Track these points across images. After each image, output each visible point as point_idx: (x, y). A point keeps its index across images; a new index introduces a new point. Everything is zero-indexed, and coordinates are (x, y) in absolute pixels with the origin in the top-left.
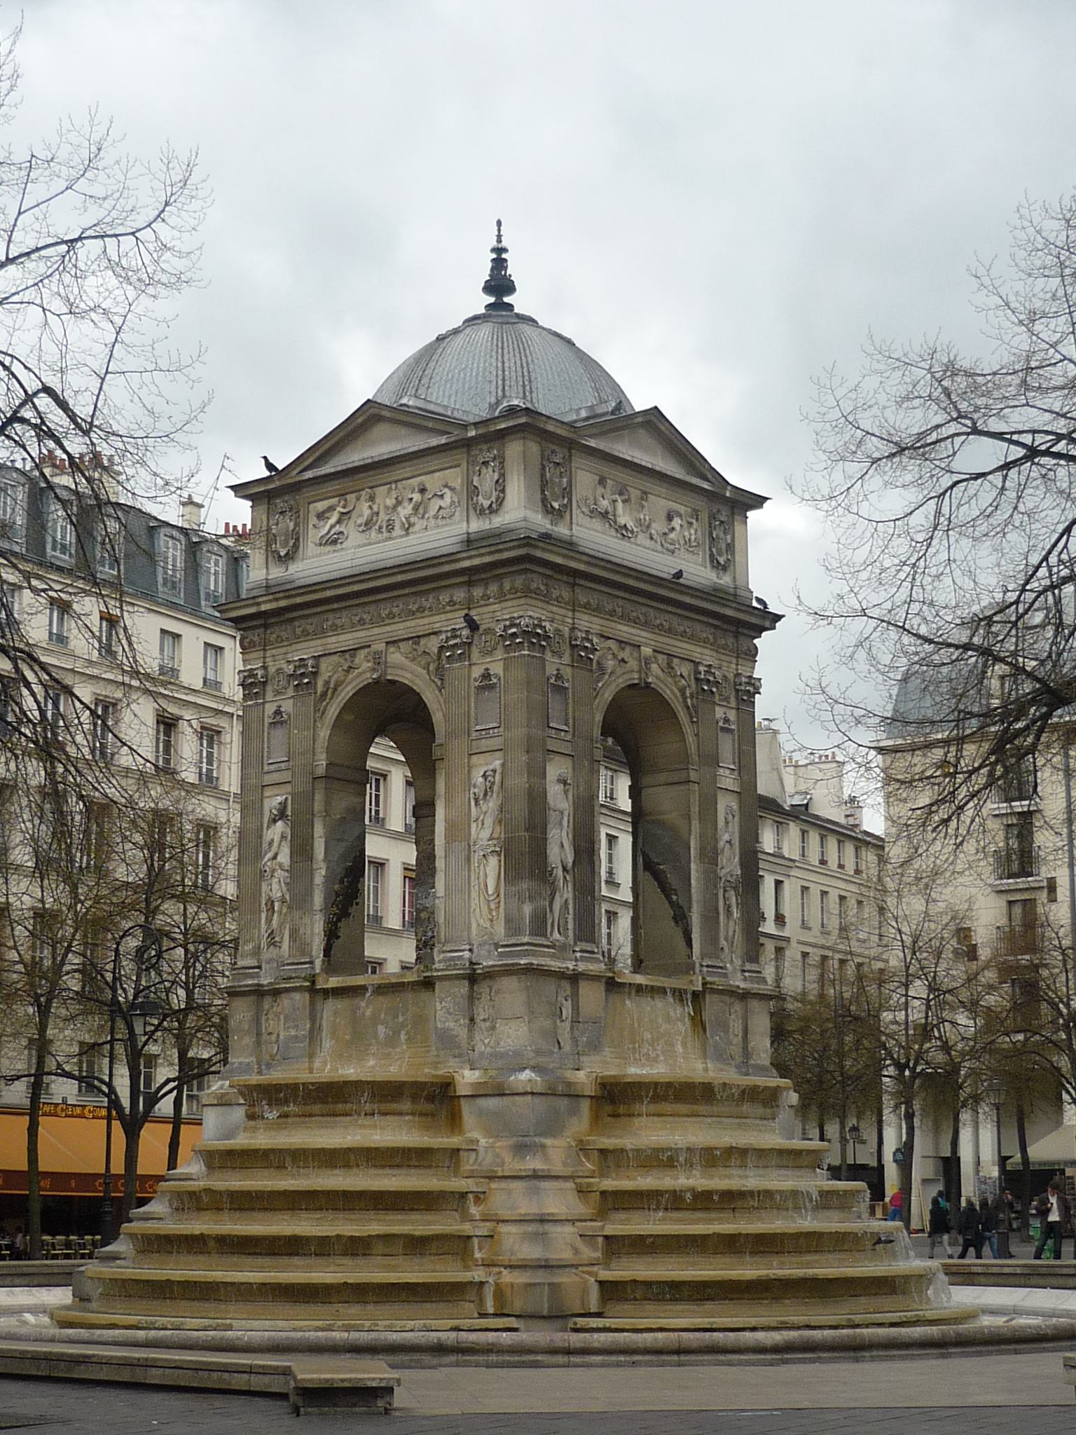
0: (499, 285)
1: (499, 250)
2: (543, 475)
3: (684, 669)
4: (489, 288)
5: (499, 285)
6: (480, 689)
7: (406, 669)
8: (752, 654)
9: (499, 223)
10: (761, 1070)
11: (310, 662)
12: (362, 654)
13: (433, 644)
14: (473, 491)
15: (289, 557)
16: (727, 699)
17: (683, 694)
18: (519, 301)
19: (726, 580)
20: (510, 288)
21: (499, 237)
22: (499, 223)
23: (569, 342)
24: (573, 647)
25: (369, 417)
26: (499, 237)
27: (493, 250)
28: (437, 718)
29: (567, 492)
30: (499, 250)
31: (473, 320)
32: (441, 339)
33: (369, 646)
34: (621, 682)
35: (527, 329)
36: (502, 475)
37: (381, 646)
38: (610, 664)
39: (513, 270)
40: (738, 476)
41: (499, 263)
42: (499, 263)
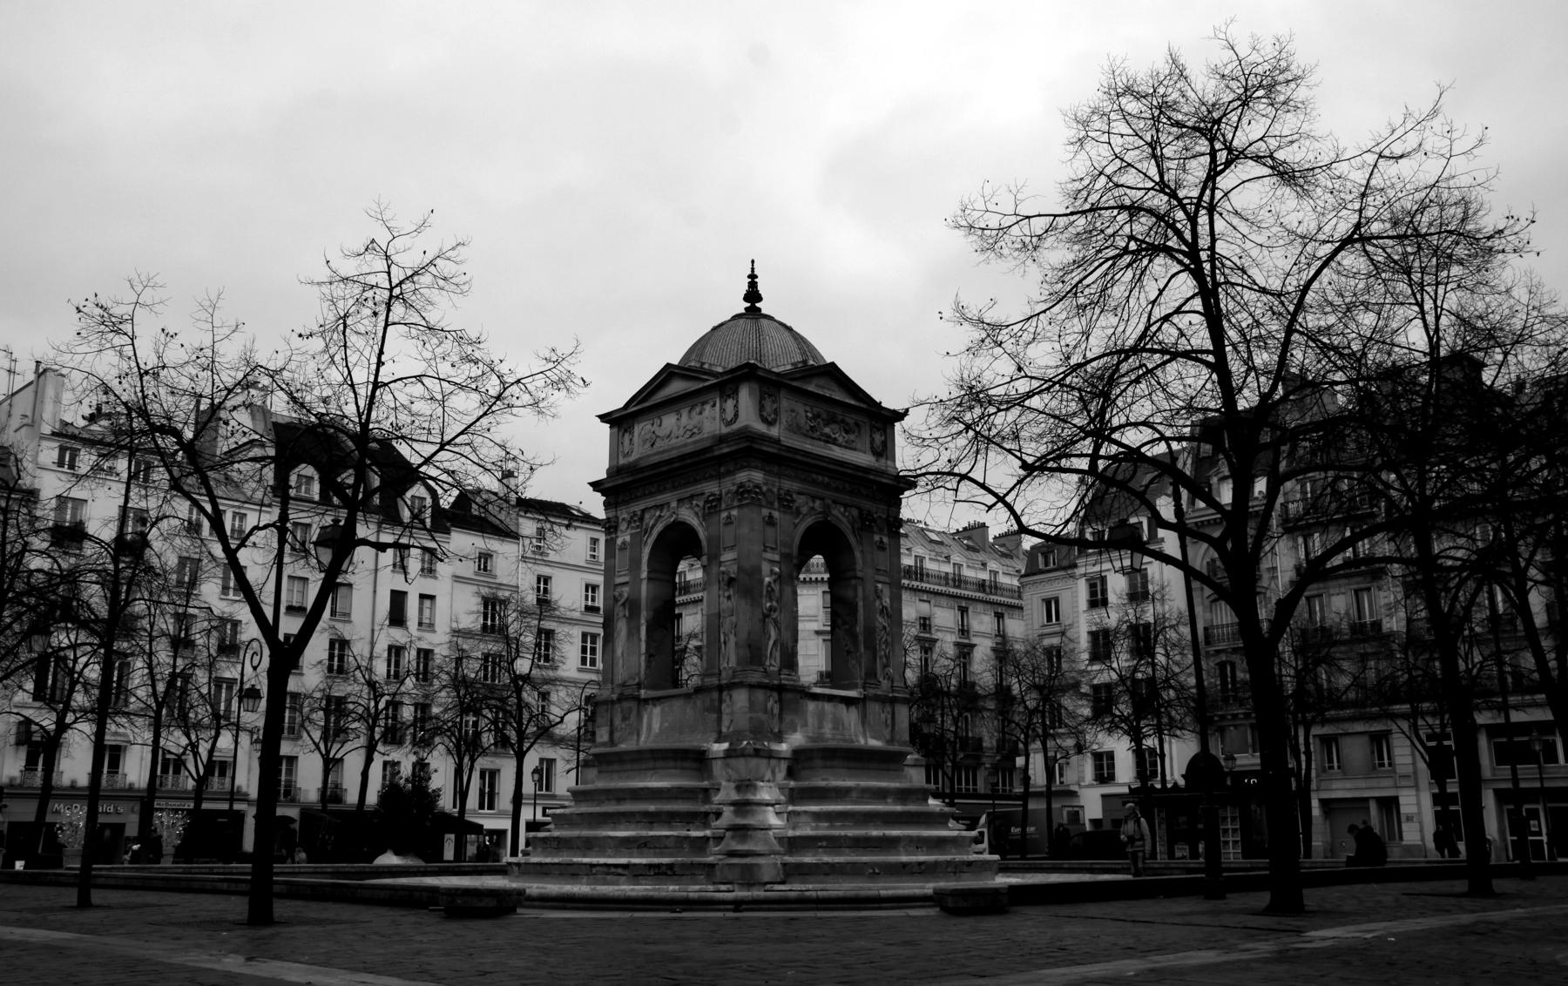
0: (753, 295)
1: (753, 276)
3: (855, 512)
4: (746, 299)
5: (753, 295)
7: (688, 515)
14: (723, 410)
18: (765, 307)
20: (760, 299)
23: (789, 329)
25: (668, 373)
29: (776, 412)
30: (753, 276)
31: (737, 317)
32: (715, 329)
35: (764, 322)
37: (674, 504)
38: (804, 510)
39: (761, 289)
41: (753, 284)
42: (753, 284)
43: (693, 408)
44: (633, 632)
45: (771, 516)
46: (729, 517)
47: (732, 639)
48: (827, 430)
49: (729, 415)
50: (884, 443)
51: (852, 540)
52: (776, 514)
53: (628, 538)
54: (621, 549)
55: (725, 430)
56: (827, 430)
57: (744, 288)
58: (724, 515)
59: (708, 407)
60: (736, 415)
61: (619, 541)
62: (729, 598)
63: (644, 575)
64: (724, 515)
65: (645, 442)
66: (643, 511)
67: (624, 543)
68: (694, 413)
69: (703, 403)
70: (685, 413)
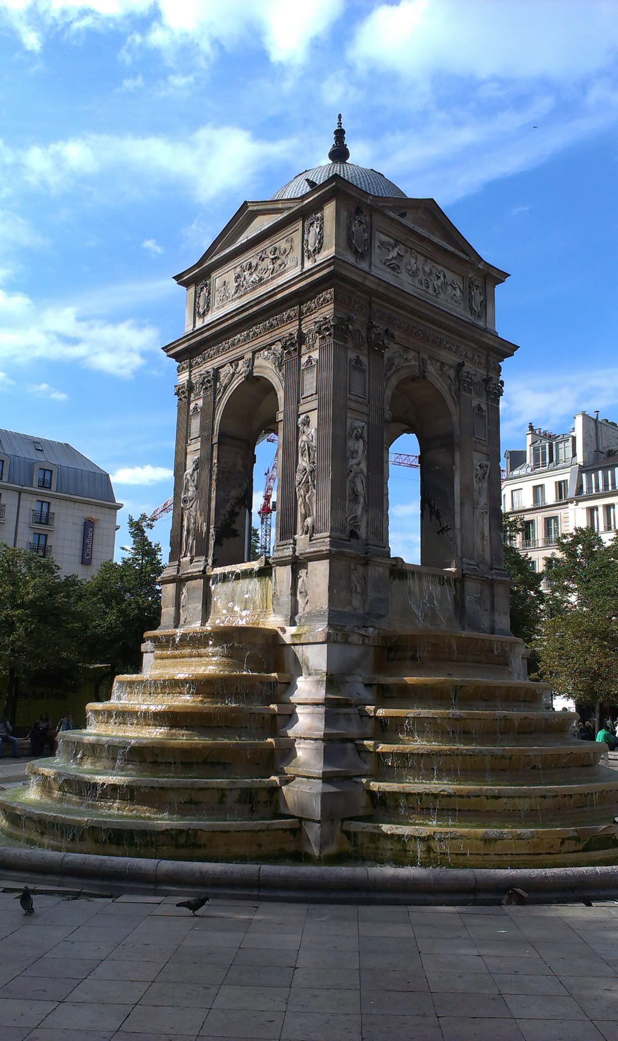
2: (349, 228)
7: (266, 366)
8: (499, 369)
9: (340, 117)
10: (502, 632)
12: (241, 363)
13: (278, 347)
15: (204, 314)
16: (481, 396)
17: (450, 389)
19: (481, 323)
21: (340, 124)
22: (340, 117)
24: (369, 342)
26: (340, 124)
27: (336, 132)
28: (281, 394)
33: (243, 358)
34: (404, 373)
40: (489, 254)
45: (358, 361)
50: (484, 305)
51: (450, 402)
52: (364, 360)
57: (329, 143)
60: (321, 243)
63: (215, 440)
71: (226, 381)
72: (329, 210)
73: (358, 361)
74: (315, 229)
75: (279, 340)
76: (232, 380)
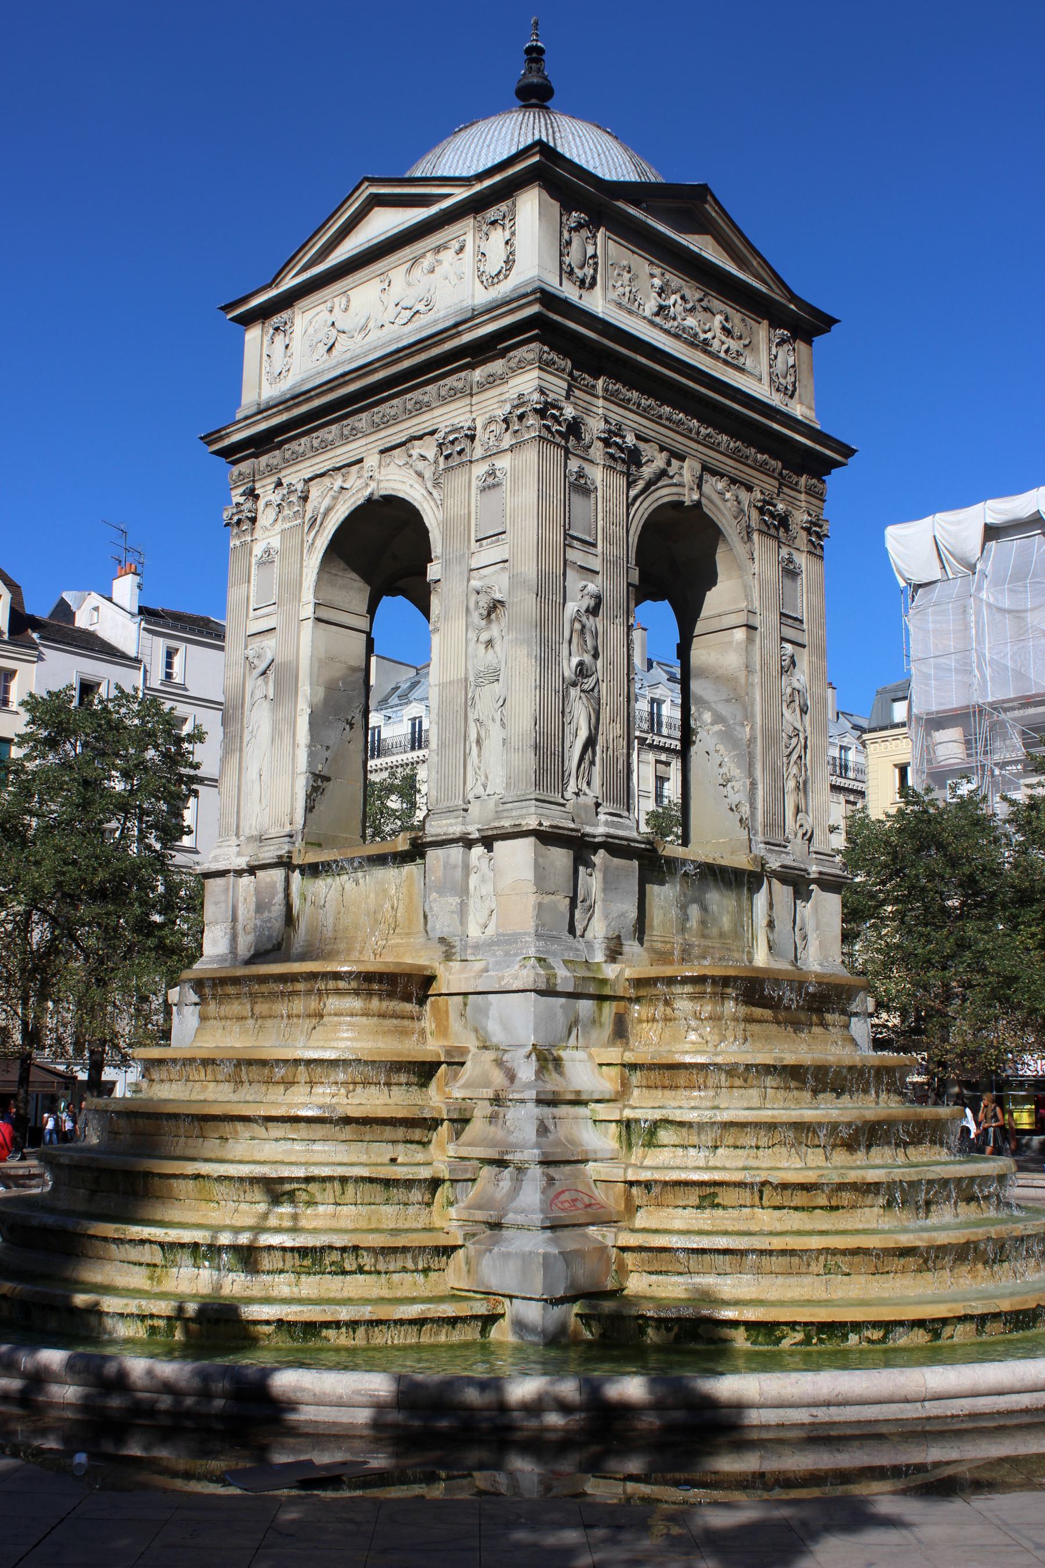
6: (483, 490)
11: (300, 486)
36: (513, 234)
39: (551, 70)
43: (416, 261)
44: (281, 729)
46: (492, 473)
47: (495, 735)
48: (690, 321)
49: (495, 263)
53: (276, 542)
54: (261, 564)
55: (483, 297)
56: (690, 321)
58: (480, 470)
59: (448, 256)
60: (510, 261)
61: (258, 549)
62: (489, 643)
63: (308, 611)
64: (480, 470)
65: (313, 348)
66: (307, 481)
67: (267, 551)
68: (417, 272)
69: (438, 250)
70: (398, 275)
71: (327, 502)
72: (530, 206)
73: (581, 474)
74: (498, 236)
75: (433, 433)
76: (336, 504)
